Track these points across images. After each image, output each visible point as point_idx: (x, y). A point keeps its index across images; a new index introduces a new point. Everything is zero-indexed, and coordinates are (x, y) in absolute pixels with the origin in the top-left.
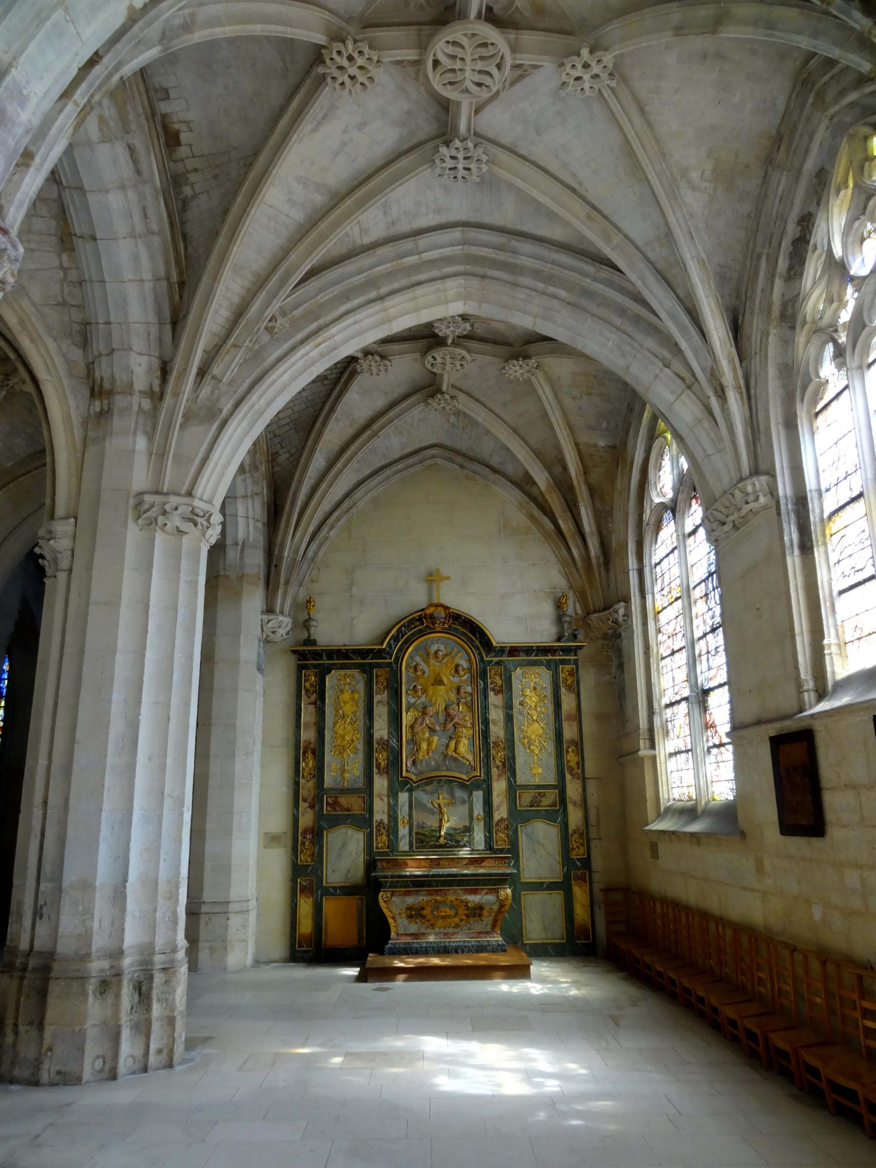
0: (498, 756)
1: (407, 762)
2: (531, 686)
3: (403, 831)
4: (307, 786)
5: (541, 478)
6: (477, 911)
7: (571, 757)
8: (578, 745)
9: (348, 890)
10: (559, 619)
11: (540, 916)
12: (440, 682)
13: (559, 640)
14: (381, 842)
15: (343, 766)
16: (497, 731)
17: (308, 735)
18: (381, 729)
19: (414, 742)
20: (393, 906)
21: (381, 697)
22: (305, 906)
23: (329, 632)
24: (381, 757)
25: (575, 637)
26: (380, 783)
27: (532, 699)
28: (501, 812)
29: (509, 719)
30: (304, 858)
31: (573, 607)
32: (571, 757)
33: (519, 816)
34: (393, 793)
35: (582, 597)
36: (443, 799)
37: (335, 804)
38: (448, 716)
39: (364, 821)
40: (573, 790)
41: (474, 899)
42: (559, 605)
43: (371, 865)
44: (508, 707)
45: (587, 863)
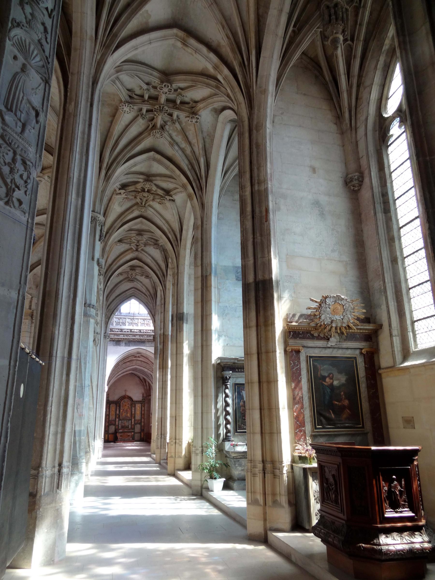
0: (133, 416)
1: (121, 417)
2: (138, 406)
3: (120, 426)
4: (107, 420)
5: (142, 378)
6: (129, 436)
7: (143, 416)
8: (144, 414)
9: (112, 434)
10: (143, 397)
11: (137, 436)
12: (126, 406)
13: (143, 400)
14: (117, 427)
15: (112, 417)
16: (133, 412)
17: (108, 413)
18: (118, 412)
19: (122, 414)
20: (119, 435)
21: (118, 408)
22: (107, 436)
23: (111, 399)
24: (117, 416)
25: (145, 400)
26: (117, 420)
27: (138, 408)
28: (133, 423)
29: (135, 411)
30: (107, 430)
31: (145, 395)
32: (143, 416)
33: (135, 424)
34: (119, 421)
35: (146, 394)
36: (125, 422)
37: (111, 422)
38: (127, 411)
39: (115, 425)
40: (143, 420)
41: (129, 434)
42: (143, 395)
43: (115, 430)
44: (135, 409)
45: (144, 430)
